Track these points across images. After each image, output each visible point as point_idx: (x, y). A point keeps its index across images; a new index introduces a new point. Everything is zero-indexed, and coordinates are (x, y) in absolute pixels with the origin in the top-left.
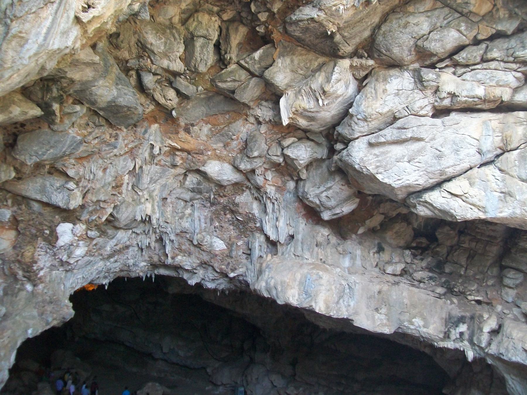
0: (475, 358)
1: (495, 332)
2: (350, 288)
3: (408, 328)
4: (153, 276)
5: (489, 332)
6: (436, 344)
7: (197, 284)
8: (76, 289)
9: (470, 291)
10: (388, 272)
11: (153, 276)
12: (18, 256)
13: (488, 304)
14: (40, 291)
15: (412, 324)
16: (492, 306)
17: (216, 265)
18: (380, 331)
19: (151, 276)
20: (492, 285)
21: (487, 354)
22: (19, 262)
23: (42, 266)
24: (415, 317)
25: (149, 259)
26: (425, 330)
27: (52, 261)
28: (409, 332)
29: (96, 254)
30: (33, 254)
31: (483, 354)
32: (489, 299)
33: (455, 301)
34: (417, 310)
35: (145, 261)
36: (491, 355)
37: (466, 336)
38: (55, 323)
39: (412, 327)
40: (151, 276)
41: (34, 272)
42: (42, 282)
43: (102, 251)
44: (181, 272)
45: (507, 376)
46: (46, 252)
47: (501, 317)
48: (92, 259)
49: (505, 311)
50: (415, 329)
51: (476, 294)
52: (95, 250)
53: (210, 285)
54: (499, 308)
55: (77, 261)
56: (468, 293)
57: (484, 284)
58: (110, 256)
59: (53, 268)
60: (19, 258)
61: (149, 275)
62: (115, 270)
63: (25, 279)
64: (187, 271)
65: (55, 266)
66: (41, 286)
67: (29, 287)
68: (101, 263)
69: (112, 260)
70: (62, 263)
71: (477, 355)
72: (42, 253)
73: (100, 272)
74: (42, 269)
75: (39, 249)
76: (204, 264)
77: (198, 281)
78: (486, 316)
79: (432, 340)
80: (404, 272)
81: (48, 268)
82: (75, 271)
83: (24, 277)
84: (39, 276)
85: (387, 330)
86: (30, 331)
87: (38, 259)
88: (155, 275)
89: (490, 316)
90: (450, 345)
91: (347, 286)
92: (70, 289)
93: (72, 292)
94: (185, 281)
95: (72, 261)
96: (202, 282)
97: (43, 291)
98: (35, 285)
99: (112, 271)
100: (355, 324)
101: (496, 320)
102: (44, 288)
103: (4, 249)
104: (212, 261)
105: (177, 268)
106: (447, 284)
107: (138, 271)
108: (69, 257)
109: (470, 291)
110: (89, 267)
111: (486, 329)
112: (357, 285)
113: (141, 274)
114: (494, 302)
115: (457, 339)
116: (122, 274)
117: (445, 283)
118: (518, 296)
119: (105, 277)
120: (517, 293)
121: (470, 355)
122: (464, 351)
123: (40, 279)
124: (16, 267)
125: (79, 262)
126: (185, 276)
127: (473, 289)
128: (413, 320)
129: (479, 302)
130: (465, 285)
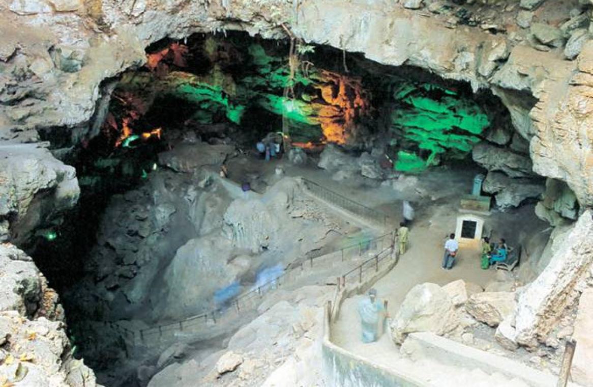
0: (480, 89)
1: (502, 61)
2: (365, 22)
3: (417, 60)
4: (225, 31)
5: (495, 61)
6: (443, 76)
7: (256, 35)
8: (152, 41)
9: (486, 19)
10: (406, 6)
11: (225, 31)
12: (88, 11)
13: (502, 32)
14: (115, 41)
15: (421, 55)
16: (507, 34)
17: (265, 15)
18: (389, 63)
19: (222, 30)
20: (512, 11)
21: (491, 85)
22: (90, 15)
23: (111, 20)
24: (423, 48)
25: (214, 14)
26: (433, 61)
27: (120, 14)
28: (418, 64)
29: (158, 8)
30: (100, 8)
31: (487, 86)
32: (504, 26)
33: (467, 29)
34: (425, 42)
35: (210, 16)
36: (494, 85)
37: (472, 66)
38: (128, 66)
39: (421, 59)
40: (222, 30)
41: (106, 24)
42: (115, 34)
43: (164, 6)
44: (243, 25)
45: (508, 106)
46: (111, 6)
47: (510, 45)
48: (155, 12)
49: (517, 38)
50: (424, 61)
51: (491, 22)
52: (154, 5)
53: (266, 35)
54: (512, 35)
55: (143, 13)
56: (483, 22)
57: (503, 11)
58: (174, 12)
59: (122, 21)
60: (90, 12)
61: (219, 30)
62: (185, 26)
63: (101, 31)
64: (246, 22)
65: (123, 19)
66: (115, 37)
67: (106, 37)
68: (167, 17)
69: (179, 15)
70: (130, 17)
71: (482, 87)
72: (108, 8)
73: (169, 26)
74: (113, 22)
75: (104, 4)
76: (257, 15)
77: (257, 32)
78: (495, 44)
79: (439, 72)
80: (422, 5)
81: (118, 21)
82: (144, 24)
83: (100, 29)
84: (111, 28)
85: (397, 62)
86: (106, 72)
87: (106, 13)
88: (227, 31)
89: (499, 44)
90: (455, 76)
91: (363, 22)
92: (146, 41)
93: (149, 43)
94: (247, 33)
95: (136, 15)
96: (261, 33)
97: (117, 41)
98: (109, 36)
99: (183, 26)
100: (366, 57)
101: (505, 47)
102: (117, 38)
103: (77, 6)
104: (262, 10)
105: (238, 21)
106: (462, 13)
107: (208, 26)
108: (132, 10)
109: (486, 19)
110: (156, 21)
111: (493, 57)
112: (372, 19)
113: (211, 29)
114: (508, 30)
115: (463, 70)
116: (197, 30)
117: (460, 12)
118: (535, 20)
119: (179, 32)
120: (535, 16)
121: (475, 88)
122: (470, 82)
123: (113, 30)
124: (89, 20)
125: (144, 16)
126: (248, 29)
127: (489, 17)
128: (421, 52)
129: (493, 31)
130: (483, 14)
